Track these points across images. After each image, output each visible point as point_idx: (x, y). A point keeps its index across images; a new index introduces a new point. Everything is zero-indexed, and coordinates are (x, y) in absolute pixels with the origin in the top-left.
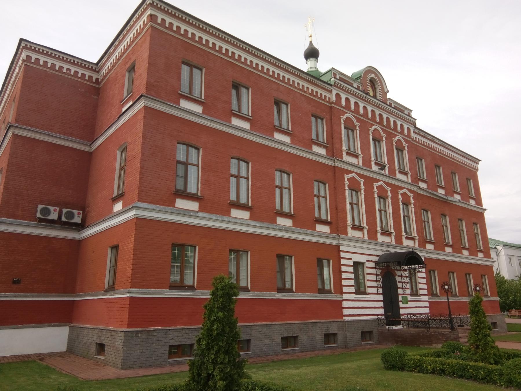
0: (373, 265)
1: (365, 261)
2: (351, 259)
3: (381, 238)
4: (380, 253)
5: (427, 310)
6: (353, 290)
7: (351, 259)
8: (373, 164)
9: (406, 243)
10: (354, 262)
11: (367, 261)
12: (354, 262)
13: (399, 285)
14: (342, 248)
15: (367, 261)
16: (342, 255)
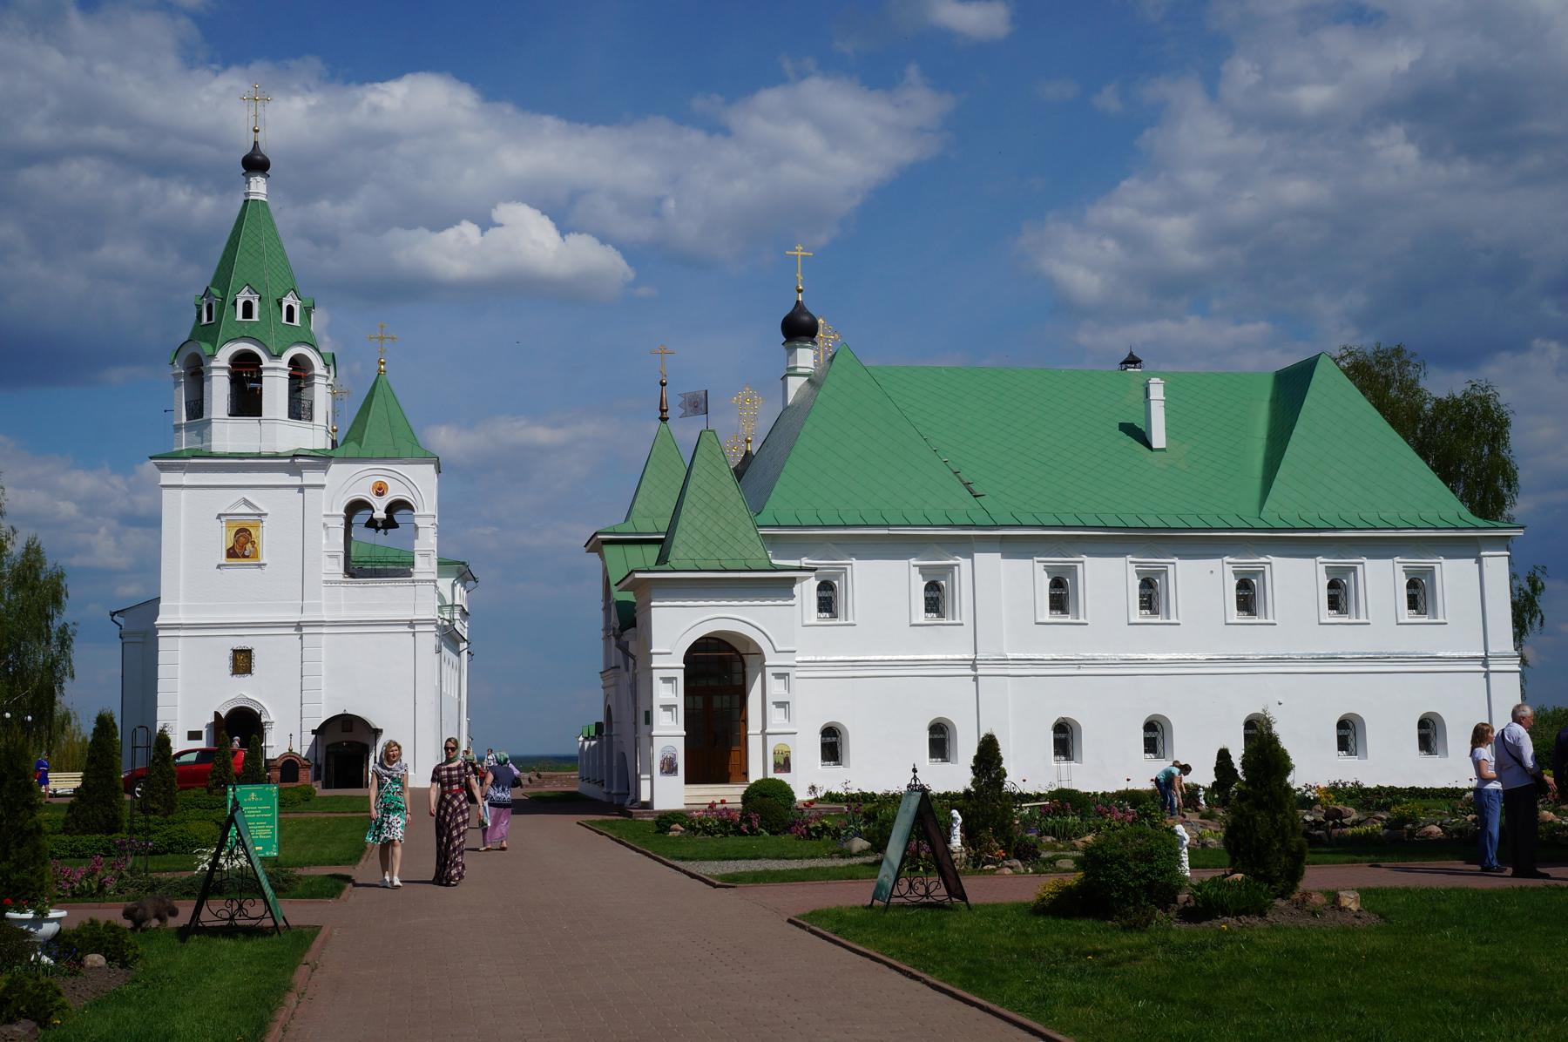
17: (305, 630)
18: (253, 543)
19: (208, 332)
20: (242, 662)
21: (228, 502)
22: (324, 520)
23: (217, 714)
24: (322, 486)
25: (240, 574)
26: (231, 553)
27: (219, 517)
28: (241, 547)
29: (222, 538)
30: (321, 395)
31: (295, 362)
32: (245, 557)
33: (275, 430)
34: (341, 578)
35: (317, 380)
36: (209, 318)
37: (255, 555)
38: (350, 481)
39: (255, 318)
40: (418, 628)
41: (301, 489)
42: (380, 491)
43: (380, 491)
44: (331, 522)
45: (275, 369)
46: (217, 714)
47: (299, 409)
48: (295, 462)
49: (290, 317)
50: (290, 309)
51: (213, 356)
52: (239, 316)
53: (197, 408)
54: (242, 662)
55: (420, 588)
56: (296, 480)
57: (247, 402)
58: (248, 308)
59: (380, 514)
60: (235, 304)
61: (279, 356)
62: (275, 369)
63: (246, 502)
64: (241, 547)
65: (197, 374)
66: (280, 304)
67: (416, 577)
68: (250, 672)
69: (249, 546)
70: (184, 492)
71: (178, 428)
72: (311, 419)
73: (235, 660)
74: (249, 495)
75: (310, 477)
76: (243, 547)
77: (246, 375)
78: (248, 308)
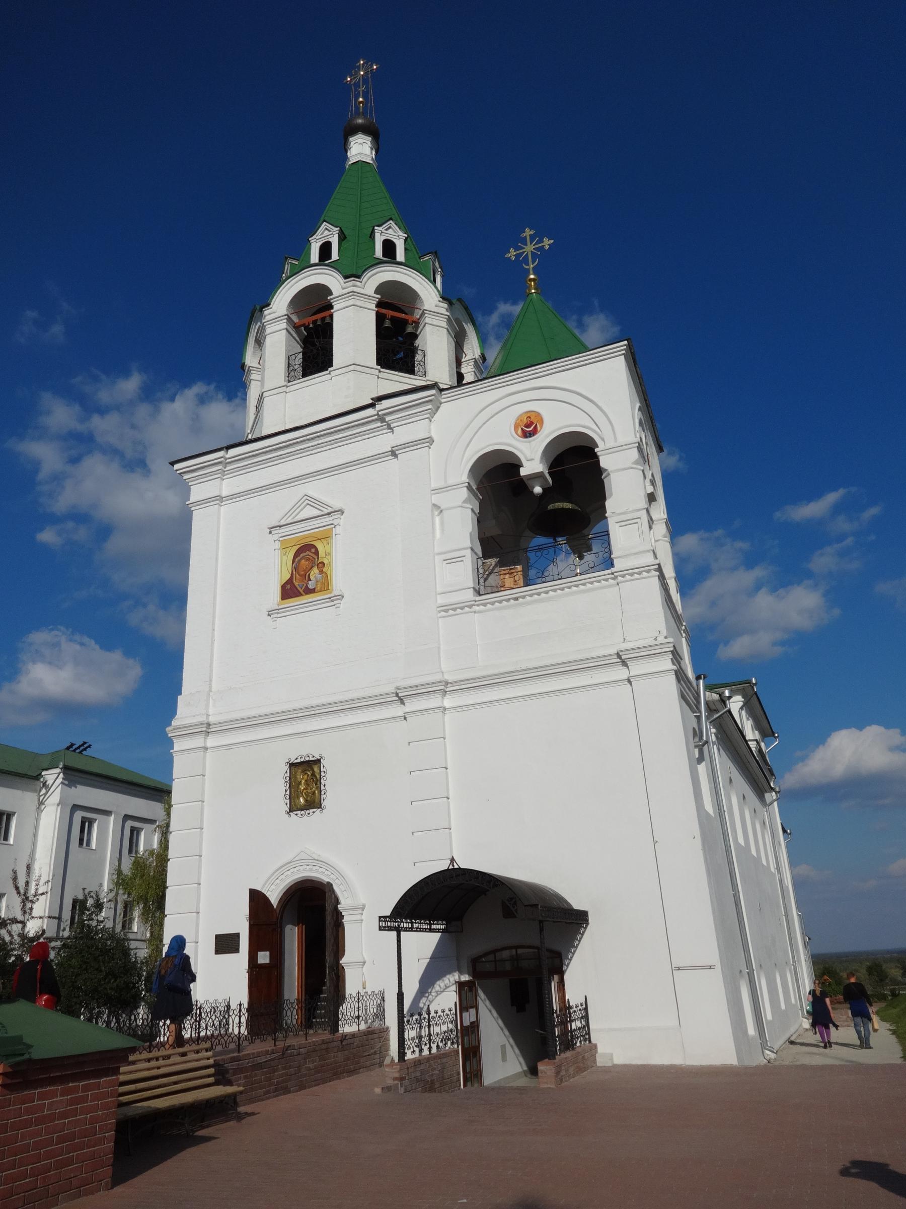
20: (305, 784)
21: (279, 505)
24: (429, 441)
26: (289, 591)
28: (304, 574)
29: (276, 568)
32: (309, 591)
34: (470, 595)
37: (325, 585)
40: (636, 668)
43: (529, 428)
46: (257, 899)
54: (305, 784)
55: (628, 587)
56: (384, 441)
57: (315, 351)
63: (310, 501)
64: (304, 574)
67: (619, 565)
68: (319, 806)
69: (315, 573)
70: (225, 509)
74: (313, 489)
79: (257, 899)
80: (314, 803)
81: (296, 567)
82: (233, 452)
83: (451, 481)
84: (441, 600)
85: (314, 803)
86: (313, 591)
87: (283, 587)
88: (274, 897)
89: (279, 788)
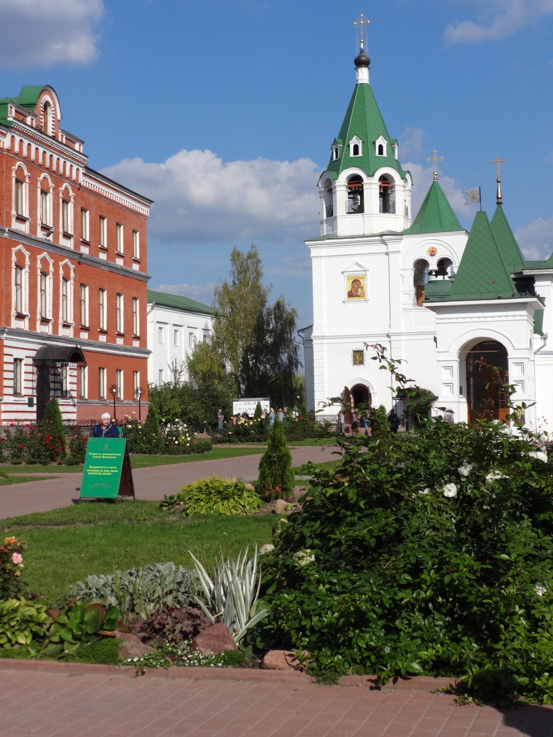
0: (30, 361)
1: (24, 357)
2: (12, 355)
3: (40, 329)
4: (38, 347)
5: (74, 417)
6: (11, 391)
7: (12, 355)
8: (39, 228)
9: (62, 332)
10: (16, 360)
11: (27, 357)
12: (16, 360)
13: (52, 386)
14: (6, 343)
15: (27, 357)
16: (6, 351)
17: (392, 338)
18: (362, 288)
19: (335, 167)
22: (401, 272)
23: (346, 388)
25: (356, 304)
27: (343, 273)
28: (356, 290)
30: (402, 196)
31: (384, 179)
32: (358, 296)
33: (374, 219)
34: (411, 306)
35: (397, 188)
36: (337, 157)
37: (363, 295)
38: (420, 247)
39: (360, 154)
41: (387, 254)
42: (433, 253)
43: (433, 253)
44: (405, 273)
45: (370, 184)
46: (346, 388)
47: (387, 206)
48: (383, 237)
49: (381, 152)
50: (381, 147)
51: (336, 179)
52: (352, 154)
53: (330, 212)
54: (358, 357)
58: (356, 147)
59: (433, 266)
60: (349, 146)
61: (373, 176)
62: (370, 184)
64: (356, 290)
65: (330, 190)
66: (374, 143)
69: (360, 290)
70: (323, 260)
71: (322, 222)
72: (394, 212)
73: (354, 357)
74: (359, 259)
75: (392, 247)
76: (356, 291)
77: (356, 187)
78: (356, 147)
79: (346, 388)
80: (361, 362)
81: (353, 287)
82: (327, 241)
83: (406, 267)
84: (402, 307)
85: (361, 362)
86: (359, 296)
87: (349, 293)
88: (350, 388)
89: (350, 358)
